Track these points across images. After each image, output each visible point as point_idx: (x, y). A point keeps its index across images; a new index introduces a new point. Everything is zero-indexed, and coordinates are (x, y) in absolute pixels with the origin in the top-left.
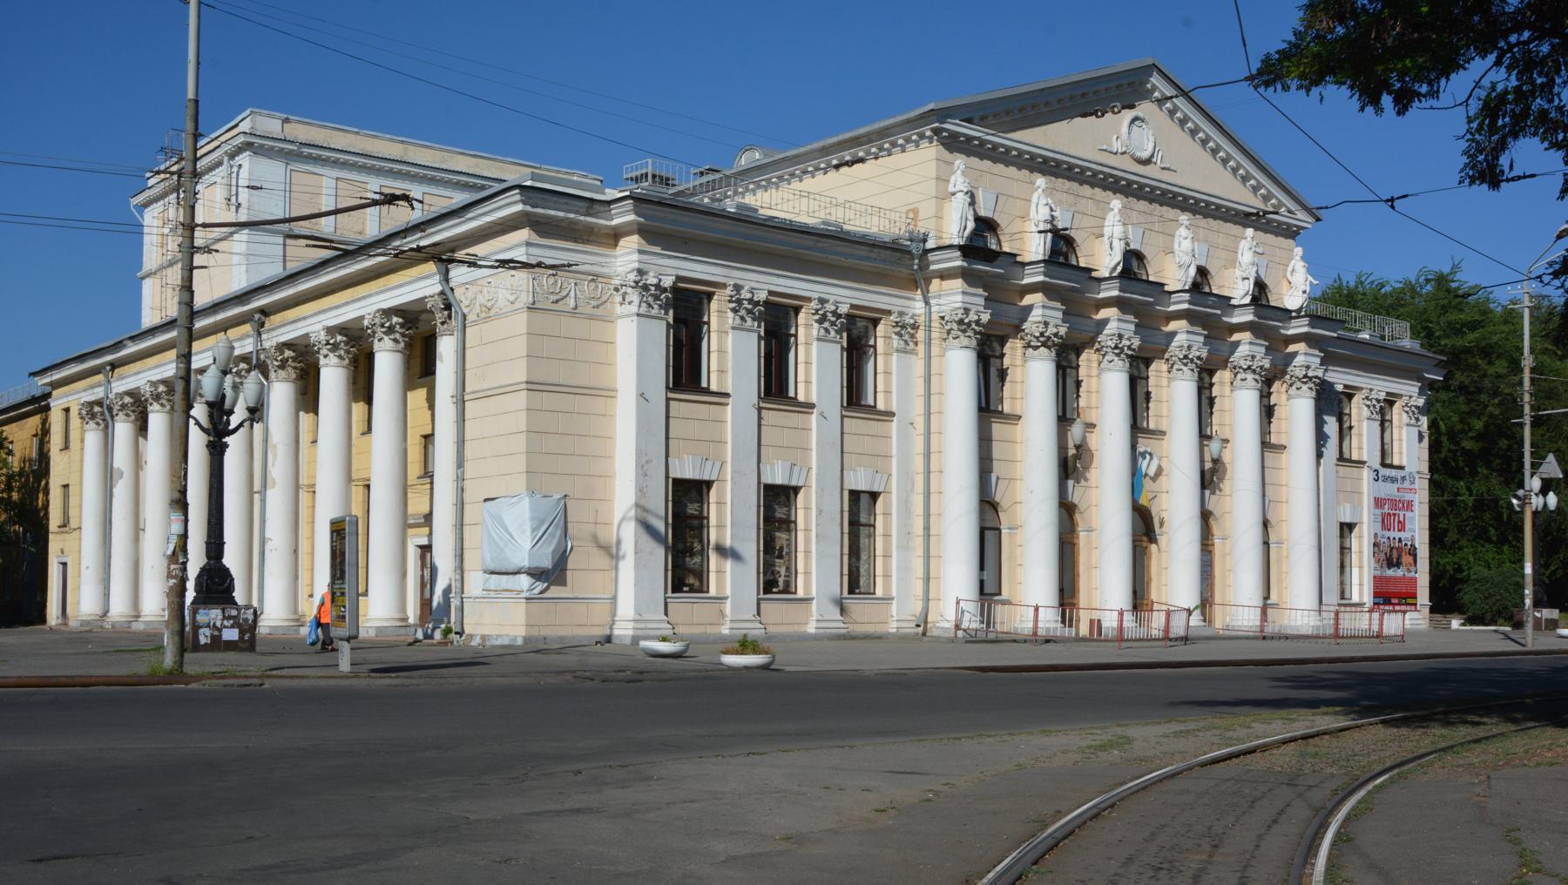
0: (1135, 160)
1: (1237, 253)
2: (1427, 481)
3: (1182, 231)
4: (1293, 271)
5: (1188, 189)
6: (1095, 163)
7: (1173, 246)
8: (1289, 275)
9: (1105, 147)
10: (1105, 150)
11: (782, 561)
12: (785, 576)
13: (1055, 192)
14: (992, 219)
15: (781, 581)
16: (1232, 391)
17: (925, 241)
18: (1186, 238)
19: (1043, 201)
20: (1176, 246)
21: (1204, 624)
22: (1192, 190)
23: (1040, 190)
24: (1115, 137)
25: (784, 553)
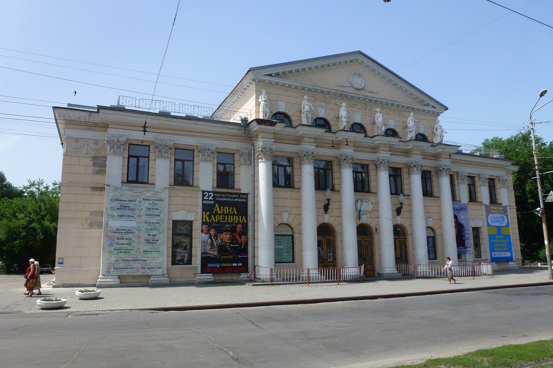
0: (356, 89)
1: (407, 123)
2: (516, 209)
3: (378, 114)
4: (436, 129)
5: (381, 99)
6: (333, 90)
7: (375, 121)
8: (435, 131)
9: (340, 85)
10: (341, 86)
11: (186, 251)
12: (188, 257)
13: (316, 102)
14: (284, 112)
15: (185, 259)
16: (409, 176)
17: (247, 121)
18: (379, 117)
19: (306, 103)
20: (376, 120)
21: (397, 272)
22: (383, 99)
23: (305, 100)
24: (345, 82)
25: (187, 248)
